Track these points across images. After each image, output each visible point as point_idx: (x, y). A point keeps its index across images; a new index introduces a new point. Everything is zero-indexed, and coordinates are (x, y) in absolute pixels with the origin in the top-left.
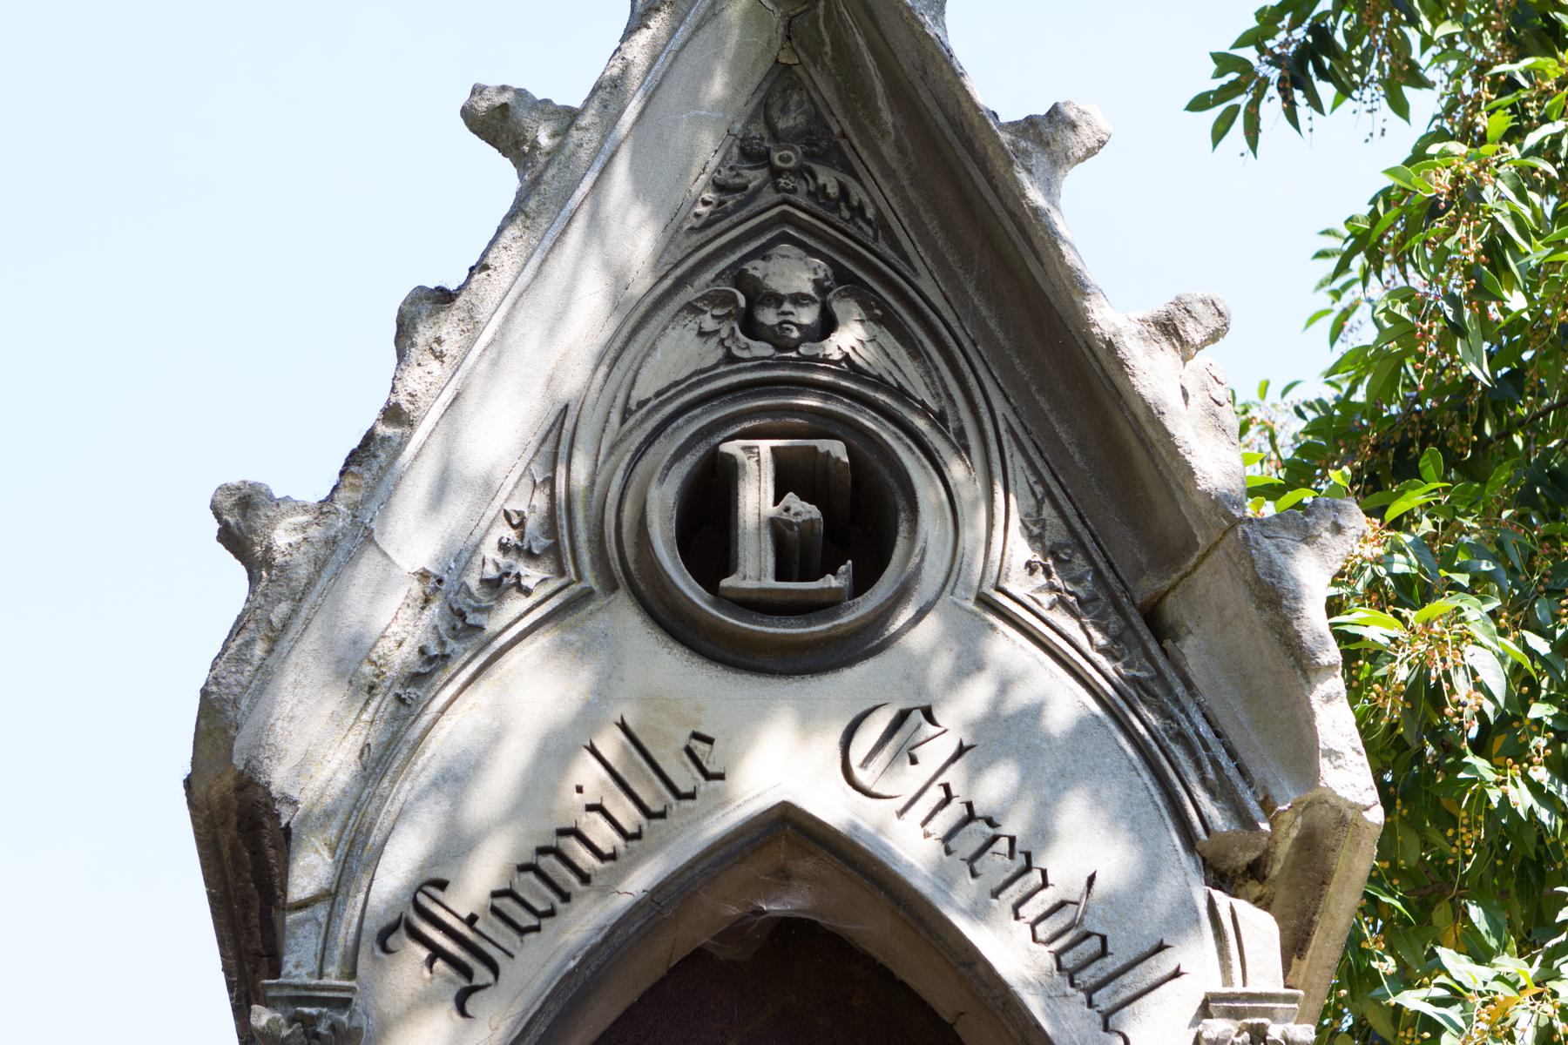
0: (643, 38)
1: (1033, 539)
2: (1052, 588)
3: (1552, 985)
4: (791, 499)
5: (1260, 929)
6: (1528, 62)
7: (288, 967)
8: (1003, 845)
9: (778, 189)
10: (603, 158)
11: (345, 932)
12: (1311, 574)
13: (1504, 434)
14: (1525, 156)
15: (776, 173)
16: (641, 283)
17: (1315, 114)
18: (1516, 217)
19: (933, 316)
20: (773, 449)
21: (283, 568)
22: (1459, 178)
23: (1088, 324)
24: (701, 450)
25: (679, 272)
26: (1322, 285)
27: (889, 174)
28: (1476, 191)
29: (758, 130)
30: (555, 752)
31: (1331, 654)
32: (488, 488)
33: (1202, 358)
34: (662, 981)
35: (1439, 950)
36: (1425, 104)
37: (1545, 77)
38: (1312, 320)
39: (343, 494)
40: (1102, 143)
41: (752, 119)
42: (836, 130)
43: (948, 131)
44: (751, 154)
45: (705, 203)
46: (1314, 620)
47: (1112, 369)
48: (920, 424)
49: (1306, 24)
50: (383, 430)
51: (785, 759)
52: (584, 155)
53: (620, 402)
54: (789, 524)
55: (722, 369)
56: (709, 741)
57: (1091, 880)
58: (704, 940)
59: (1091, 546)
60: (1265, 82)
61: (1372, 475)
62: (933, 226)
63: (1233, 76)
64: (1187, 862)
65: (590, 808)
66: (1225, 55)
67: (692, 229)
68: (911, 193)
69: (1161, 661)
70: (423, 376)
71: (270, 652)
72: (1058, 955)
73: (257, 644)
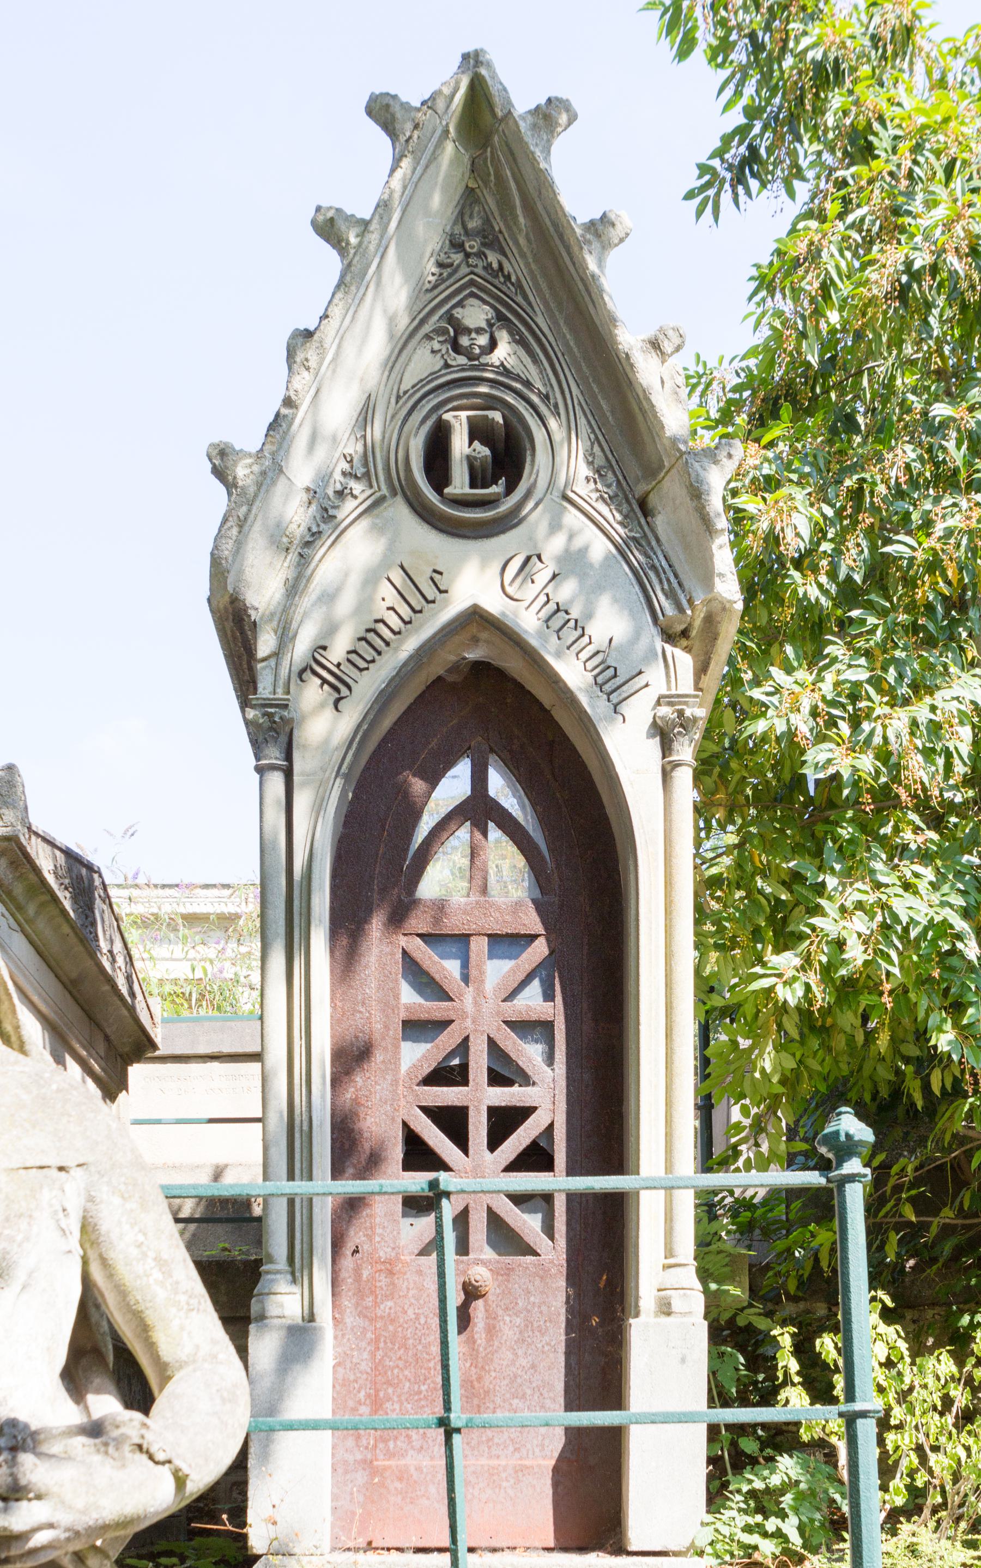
0: (399, 174)
1: (590, 463)
2: (597, 490)
3: (819, 685)
4: (476, 444)
5: (684, 661)
6: (853, 169)
7: (260, 690)
8: (572, 623)
9: (469, 266)
10: (382, 249)
11: (284, 672)
12: (716, 480)
13: (826, 392)
14: (846, 229)
15: (468, 255)
16: (403, 322)
17: (748, 200)
18: (838, 267)
19: (544, 339)
20: (468, 417)
21: (243, 488)
22: (812, 243)
23: (616, 343)
24: (434, 418)
25: (421, 316)
26: (750, 299)
27: (523, 255)
28: (819, 251)
29: (458, 229)
30: (371, 579)
31: (722, 523)
32: (334, 440)
33: (671, 361)
34: (424, 692)
35: (771, 669)
36: (802, 190)
37: (860, 178)
38: (745, 318)
39: (267, 447)
40: (627, 235)
41: (455, 224)
42: (497, 229)
43: (552, 229)
44: (456, 245)
45: (433, 274)
46: (715, 503)
47: (628, 369)
48: (535, 399)
49: (746, 144)
50: (285, 411)
51: (474, 580)
52: (372, 248)
53: (395, 392)
54: (475, 458)
55: (443, 372)
56: (441, 573)
57: (611, 640)
58: (441, 672)
59: (616, 467)
60: (723, 181)
61: (761, 416)
62: (544, 286)
63: (707, 177)
64: (654, 630)
65: (389, 609)
66: (704, 165)
67: (427, 290)
68: (533, 266)
69: (646, 528)
70: (302, 380)
71: (240, 532)
72: (595, 677)
73: (237, 522)
